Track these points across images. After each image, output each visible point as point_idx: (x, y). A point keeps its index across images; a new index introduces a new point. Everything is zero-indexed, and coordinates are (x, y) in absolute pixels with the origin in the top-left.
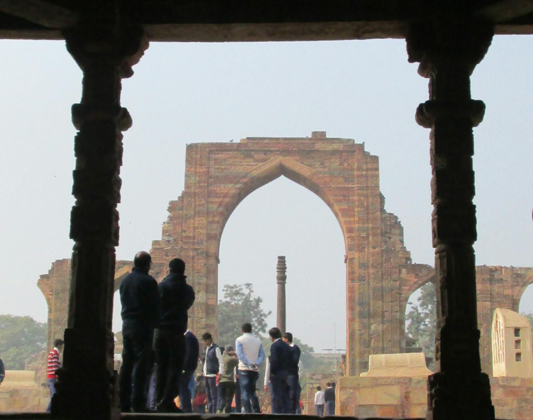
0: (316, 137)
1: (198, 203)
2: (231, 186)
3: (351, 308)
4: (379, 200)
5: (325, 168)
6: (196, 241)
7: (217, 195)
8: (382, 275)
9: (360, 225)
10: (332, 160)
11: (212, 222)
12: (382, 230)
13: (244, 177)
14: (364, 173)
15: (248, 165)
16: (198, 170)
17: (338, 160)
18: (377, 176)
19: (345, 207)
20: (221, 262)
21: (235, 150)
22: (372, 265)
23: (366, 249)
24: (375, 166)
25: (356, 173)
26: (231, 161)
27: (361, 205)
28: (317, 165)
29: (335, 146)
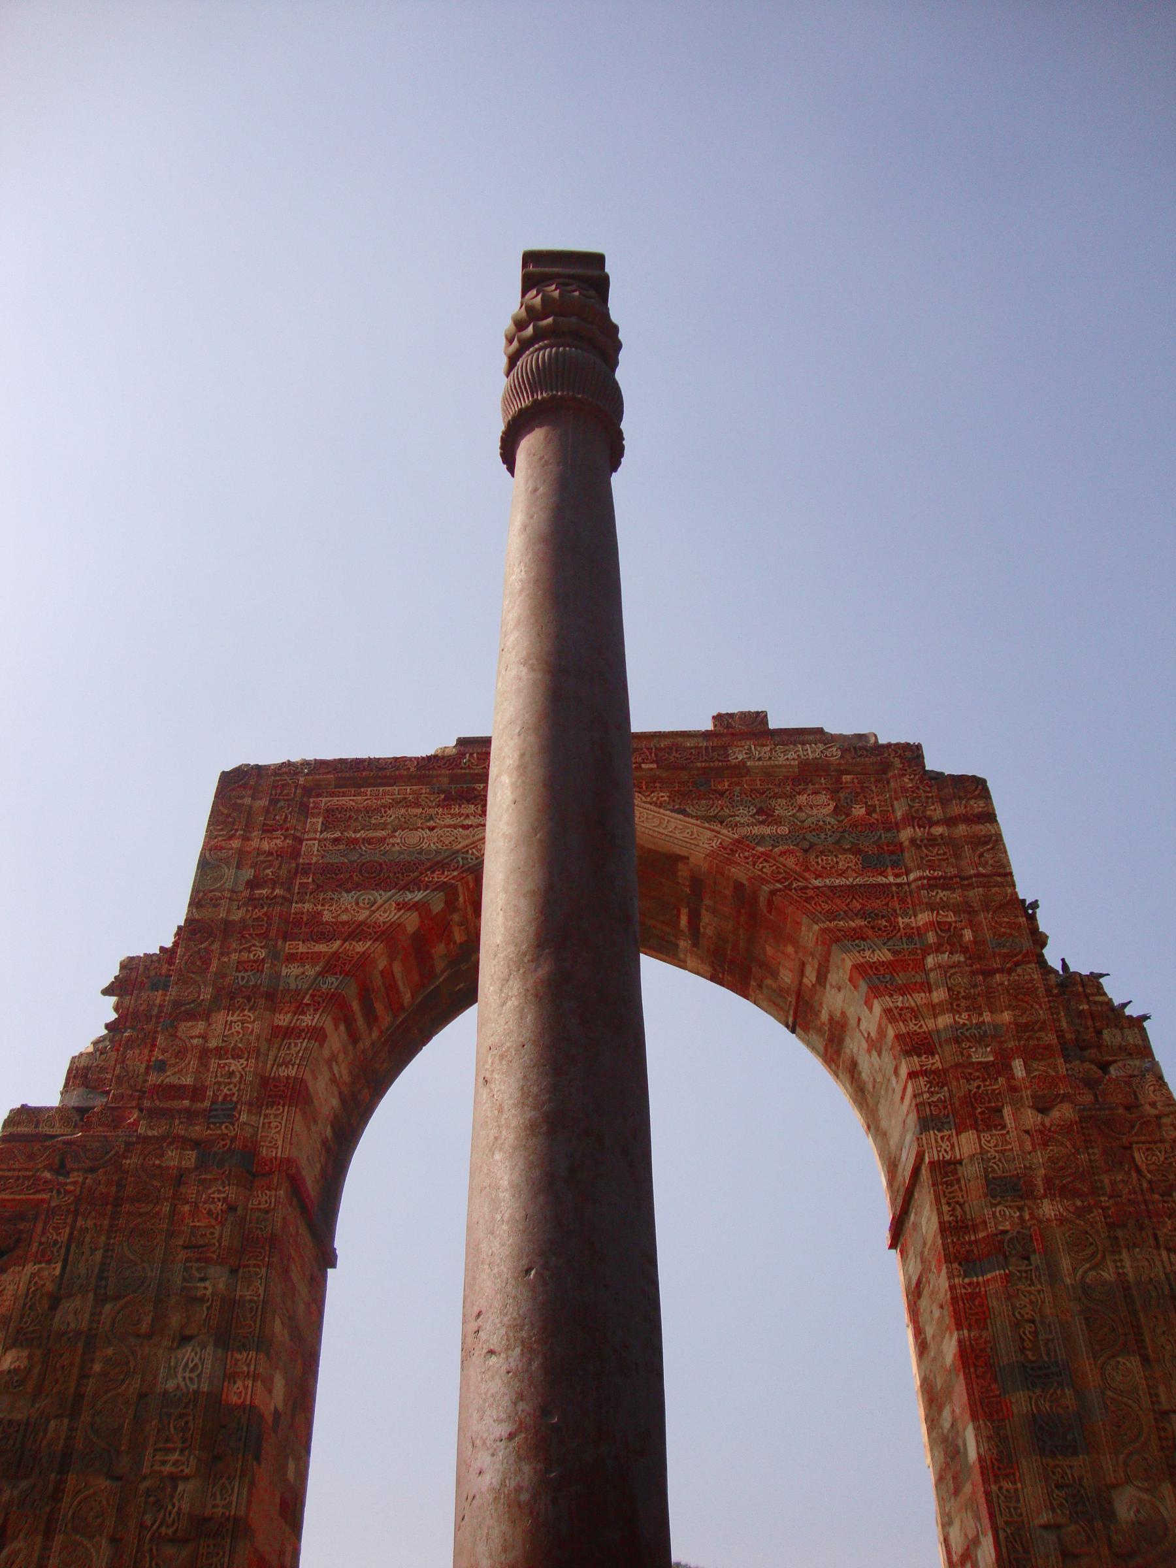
0: (729, 726)
1: (235, 957)
2: (379, 896)
3: (987, 1409)
4: (1023, 920)
5: (778, 822)
6: (207, 1104)
7: (317, 930)
8: (1110, 1226)
9: (963, 1018)
10: (802, 799)
11: (289, 1033)
12: (1060, 1034)
13: (441, 865)
14: (938, 830)
15: (455, 827)
16: (255, 843)
17: (823, 798)
18: (995, 842)
19: (883, 955)
20: (340, 1262)
21: (410, 779)
22: (1048, 1180)
23: (1007, 1111)
24: (977, 806)
25: (906, 835)
26: (394, 815)
27: (949, 939)
28: (744, 814)
29: (813, 752)
